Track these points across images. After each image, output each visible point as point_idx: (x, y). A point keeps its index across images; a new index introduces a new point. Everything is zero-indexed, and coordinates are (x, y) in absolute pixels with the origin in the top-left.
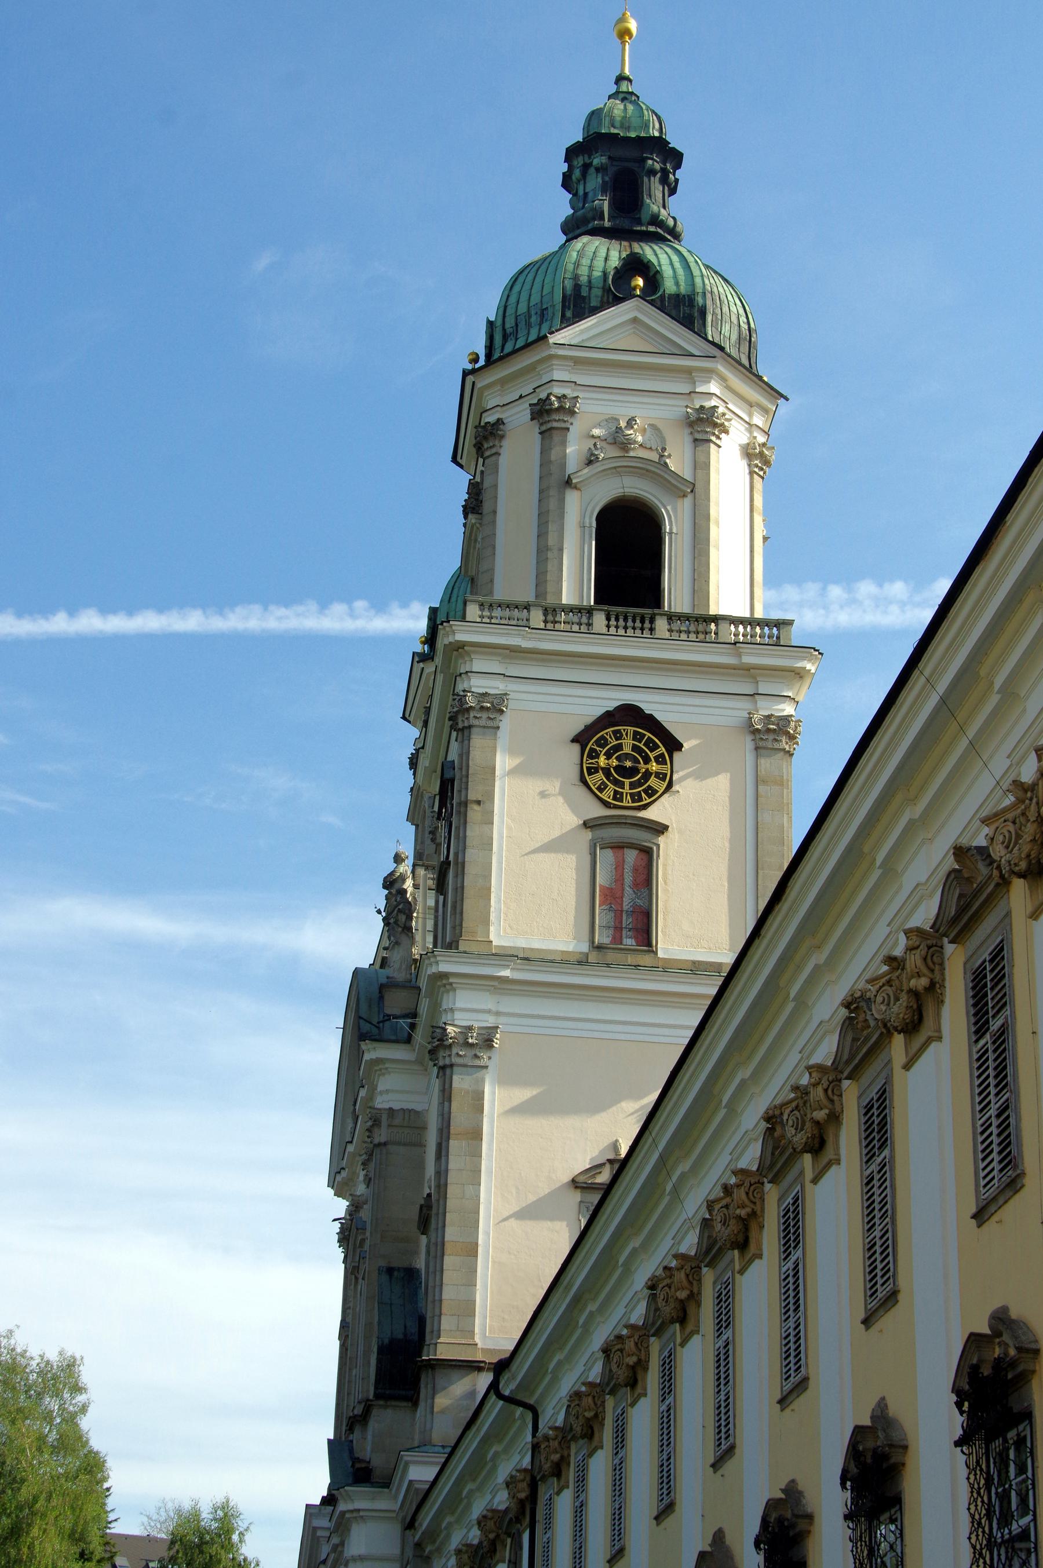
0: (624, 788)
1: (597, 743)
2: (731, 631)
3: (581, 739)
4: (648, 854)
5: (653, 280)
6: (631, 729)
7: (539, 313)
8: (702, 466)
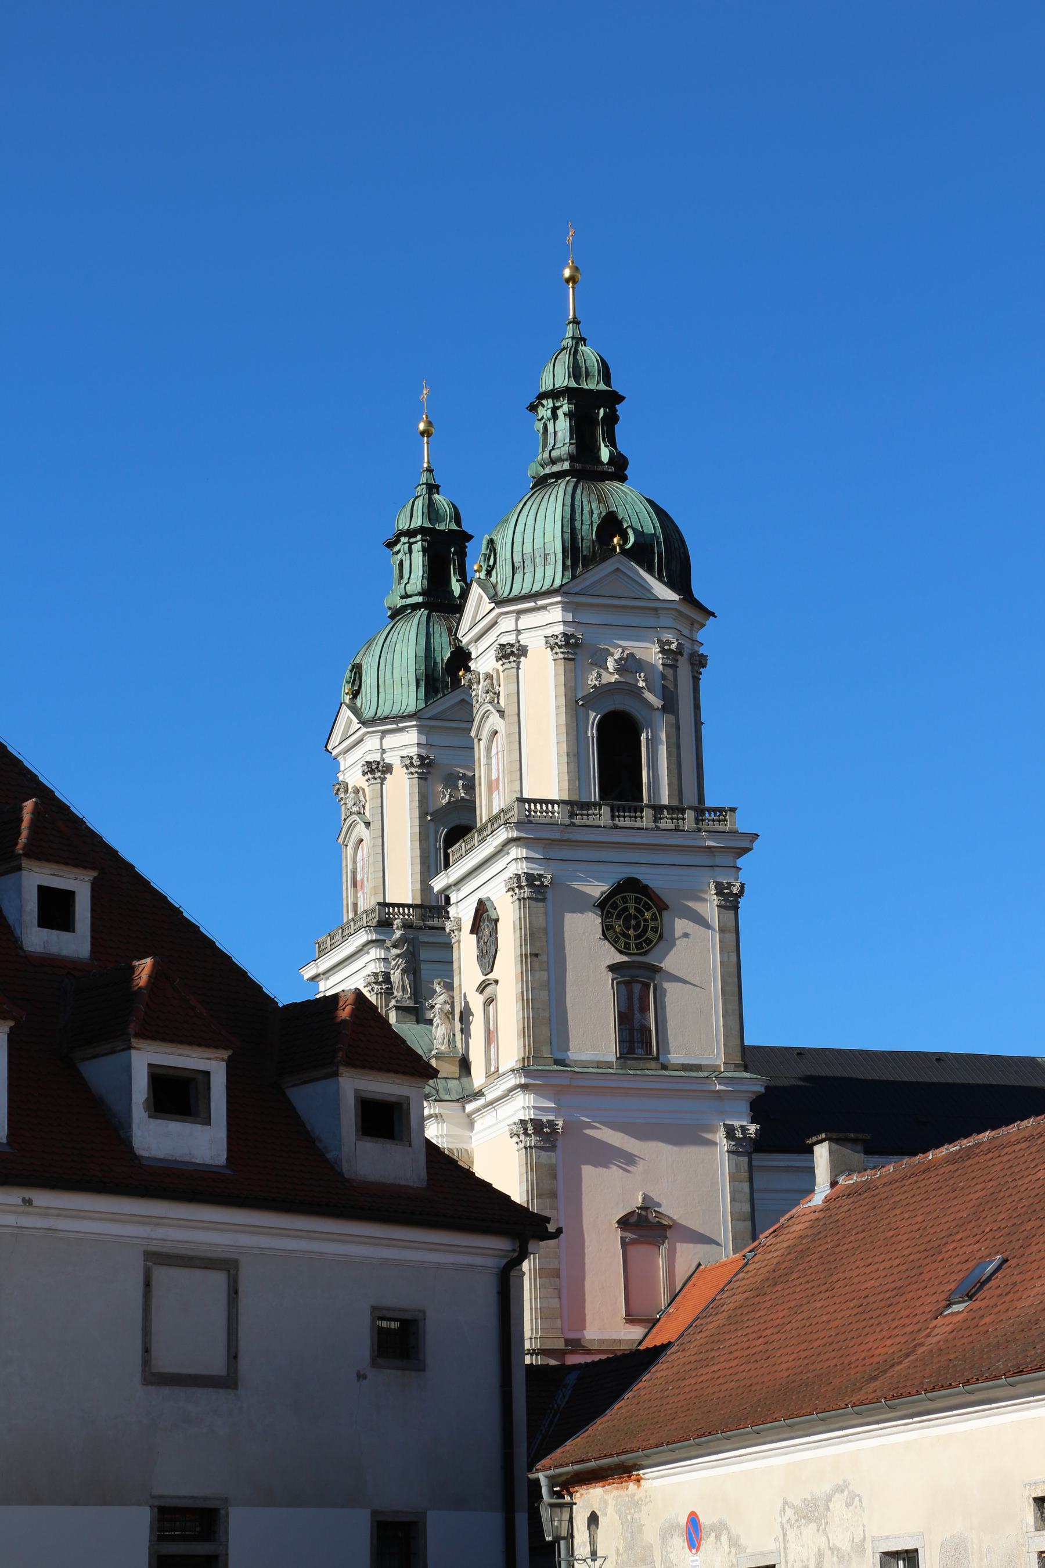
0: (630, 940)
7: (543, 556)
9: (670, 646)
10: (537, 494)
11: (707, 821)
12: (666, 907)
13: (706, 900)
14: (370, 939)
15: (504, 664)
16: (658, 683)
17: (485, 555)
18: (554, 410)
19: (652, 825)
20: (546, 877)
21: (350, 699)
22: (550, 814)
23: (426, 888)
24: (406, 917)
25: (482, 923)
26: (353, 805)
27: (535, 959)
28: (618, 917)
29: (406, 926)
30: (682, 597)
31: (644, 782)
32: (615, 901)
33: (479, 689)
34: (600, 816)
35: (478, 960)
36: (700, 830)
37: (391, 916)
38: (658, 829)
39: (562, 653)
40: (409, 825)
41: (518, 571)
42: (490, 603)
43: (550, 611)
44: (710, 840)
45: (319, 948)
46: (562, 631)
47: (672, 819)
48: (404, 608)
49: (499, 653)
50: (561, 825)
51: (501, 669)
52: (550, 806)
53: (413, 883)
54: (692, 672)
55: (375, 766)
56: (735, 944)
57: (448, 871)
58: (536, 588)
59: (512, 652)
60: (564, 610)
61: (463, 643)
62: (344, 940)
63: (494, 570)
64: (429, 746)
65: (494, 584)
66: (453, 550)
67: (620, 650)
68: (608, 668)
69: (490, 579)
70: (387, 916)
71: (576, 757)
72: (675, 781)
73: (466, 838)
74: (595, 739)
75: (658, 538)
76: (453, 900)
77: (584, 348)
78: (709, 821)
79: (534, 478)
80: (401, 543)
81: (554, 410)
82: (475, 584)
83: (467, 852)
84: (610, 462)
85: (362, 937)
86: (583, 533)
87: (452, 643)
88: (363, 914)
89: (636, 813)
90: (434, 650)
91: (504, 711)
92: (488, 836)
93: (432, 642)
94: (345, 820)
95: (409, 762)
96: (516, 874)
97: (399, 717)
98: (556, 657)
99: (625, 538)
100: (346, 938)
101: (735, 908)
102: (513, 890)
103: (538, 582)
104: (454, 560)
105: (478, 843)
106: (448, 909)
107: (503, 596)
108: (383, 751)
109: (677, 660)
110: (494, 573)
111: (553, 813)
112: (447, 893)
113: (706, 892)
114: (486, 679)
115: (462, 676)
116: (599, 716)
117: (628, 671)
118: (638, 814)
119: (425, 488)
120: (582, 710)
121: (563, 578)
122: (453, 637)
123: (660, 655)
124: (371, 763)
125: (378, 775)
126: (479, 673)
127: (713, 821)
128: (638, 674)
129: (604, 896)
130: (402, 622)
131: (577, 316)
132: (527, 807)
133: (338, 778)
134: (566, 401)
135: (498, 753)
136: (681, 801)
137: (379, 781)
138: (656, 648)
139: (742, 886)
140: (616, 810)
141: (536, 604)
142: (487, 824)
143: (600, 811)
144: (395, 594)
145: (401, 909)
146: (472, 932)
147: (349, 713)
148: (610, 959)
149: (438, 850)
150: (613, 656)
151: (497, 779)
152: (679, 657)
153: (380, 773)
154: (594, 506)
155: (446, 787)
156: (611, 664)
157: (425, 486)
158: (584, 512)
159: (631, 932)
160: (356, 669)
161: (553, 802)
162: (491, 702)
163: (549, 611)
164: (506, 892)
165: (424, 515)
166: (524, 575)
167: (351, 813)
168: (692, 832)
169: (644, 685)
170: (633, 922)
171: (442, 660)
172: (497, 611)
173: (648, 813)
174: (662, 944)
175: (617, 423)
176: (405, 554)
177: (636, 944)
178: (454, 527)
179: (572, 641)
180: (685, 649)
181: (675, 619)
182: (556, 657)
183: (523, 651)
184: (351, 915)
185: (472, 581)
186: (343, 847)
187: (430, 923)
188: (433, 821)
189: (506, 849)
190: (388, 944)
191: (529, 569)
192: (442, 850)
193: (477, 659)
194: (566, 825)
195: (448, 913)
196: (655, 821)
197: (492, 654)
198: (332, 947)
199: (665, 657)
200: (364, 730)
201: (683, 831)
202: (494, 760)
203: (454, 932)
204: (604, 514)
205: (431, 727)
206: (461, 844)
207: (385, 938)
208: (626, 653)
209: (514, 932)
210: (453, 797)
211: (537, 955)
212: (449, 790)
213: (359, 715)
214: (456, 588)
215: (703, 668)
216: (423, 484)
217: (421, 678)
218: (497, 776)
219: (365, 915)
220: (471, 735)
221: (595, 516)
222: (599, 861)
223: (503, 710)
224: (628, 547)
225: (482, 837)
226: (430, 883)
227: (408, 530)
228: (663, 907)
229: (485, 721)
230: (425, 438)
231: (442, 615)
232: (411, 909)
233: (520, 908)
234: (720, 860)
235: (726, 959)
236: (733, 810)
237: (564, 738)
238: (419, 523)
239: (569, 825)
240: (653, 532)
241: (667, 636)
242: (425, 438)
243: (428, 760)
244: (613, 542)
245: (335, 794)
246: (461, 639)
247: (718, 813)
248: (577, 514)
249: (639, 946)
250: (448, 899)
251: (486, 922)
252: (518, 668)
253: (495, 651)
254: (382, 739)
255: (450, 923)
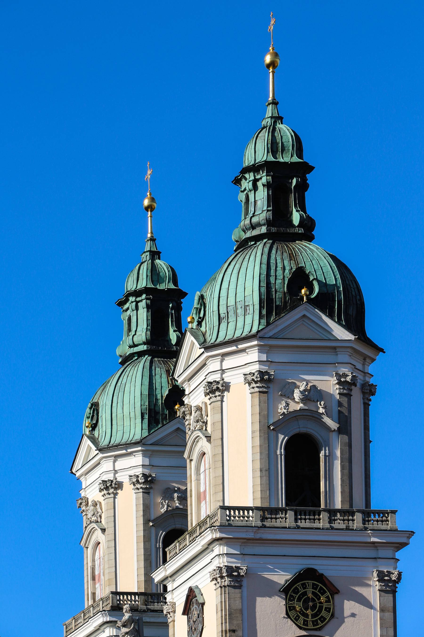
0: (308, 618)
1: (294, 591)
6: (310, 582)
7: (243, 307)
9: (345, 378)
10: (239, 255)
11: (372, 521)
12: (337, 592)
13: (369, 586)
14: (105, 621)
15: (211, 398)
16: (335, 409)
17: (197, 308)
18: (255, 182)
19: (327, 525)
20: (242, 569)
21: (89, 431)
22: (246, 518)
23: (148, 579)
24: (133, 603)
25: (191, 607)
26: (93, 516)
27: (233, 634)
28: (299, 600)
29: (133, 609)
30: (357, 337)
31: (321, 490)
32: (296, 587)
33: (191, 419)
34: (286, 519)
35: (188, 635)
36: (366, 529)
37: (122, 602)
38: (332, 528)
39: (258, 387)
40: (135, 530)
41: (223, 321)
42: (200, 348)
43: (249, 353)
44: (374, 537)
45: (66, 629)
46: (258, 369)
47: (344, 520)
48: (132, 355)
49: (207, 390)
50: (255, 527)
51: (208, 402)
52: (246, 512)
53: (138, 576)
54: (363, 399)
55: (110, 484)
56: (393, 621)
57: (166, 565)
58: (238, 334)
59: (218, 388)
60: (260, 351)
61: (179, 382)
62: (85, 621)
63: (204, 321)
64: (151, 466)
65: (203, 333)
66: (171, 305)
67: (305, 383)
68: (294, 399)
69: (201, 329)
70: (118, 602)
71: (268, 472)
72: (347, 489)
73: (179, 539)
74: (283, 457)
75: (338, 288)
76: (169, 589)
77: (281, 126)
78: (374, 521)
79: (237, 241)
80: (130, 302)
81: (255, 182)
82: (189, 333)
83: (181, 550)
84: (300, 225)
85: (99, 620)
86: (276, 287)
87: (170, 382)
88: (100, 601)
89: (314, 516)
90: (156, 389)
91: (211, 437)
92: (197, 537)
93: (154, 382)
94: (86, 527)
95: (135, 480)
96: (219, 567)
97: (128, 444)
98: (253, 390)
99: (311, 289)
100: (87, 620)
101: (394, 592)
102: (216, 580)
103: (239, 329)
104: (172, 314)
105: (189, 542)
106: (166, 596)
107: (210, 343)
108: (116, 472)
109: (351, 390)
110: (203, 324)
111: (248, 517)
112: (165, 583)
113: (370, 579)
114: (196, 411)
115: (178, 409)
116: (287, 438)
117: (311, 400)
118: (317, 517)
119: (149, 255)
120: (273, 434)
121: (259, 325)
122: (171, 378)
123: (338, 386)
124: (106, 481)
125: (111, 491)
126: (191, 406)
127: (377, 521)
128: (319, 403)
129: (288, 583)
130: (131, 367)
131: (275, 98)
132: (228, 513)
133: (81, 494)
134: (265, 174)
135: (205, 470)
136: (351, 505)
137: (112, 495)
138: (334, 380)
139: (400, 574)
140: (298, 514)
141: (237, 347)
142: (196, 527)
143: (285, 515)
144: (125, 344)
145: (129, 596)
146: (184, 613)
147: (89, 442)
148: (291, 633)
149: (157, 549)
150: (299, 388)
151: (205, 492)
152: (353, 387)
153: (113, 489)
154: (286, 263)
155: (164, 498)
156: (297, 395)
157: (148, 253)
158: (278, 269)
159: (309, 612)
160: (95, 407)
161: (248, 509)
162: (200, 430)
163: (248, 354)
164: (211, 581)
165: (148, 278)
166: (228, 324)
167: (91, 522)
168: (360, 530)
169: (324, 411)
170: (311, 604)
171: (162, 396)
172: (206, 355)
173: (324, 516)
174: (334, 621)
175: (306, 190)
176: (133, 311)
177: (312, 621)
178: (172, 286)
179: (266, 377)
180: (359, 381)
181: (350, 356)
182: (253, 390)
183: (226, 387)
184: (91, 602)
185: (186, 331)
186: (85, 549)
187: (151, 607)
188: (154, 526)
189: (211, 547)
190: (119, 624)
191: (232, 319)
192: (161, 549)
193: (190, 395)
194: (258, 527)
195: (165, 598)
196: (330, 522)
197: (201, 390)
198: (76, 628)
199: (341, 387)
200: (101, 455)
201: (352, 530)
202: (202, 476)
203: (170, 614)
204: (294, 270)
205: (153, 451)
206: (176, 543)
207: (117, 620)
208: (309, 386)
209: (217, 613)
210: (170, 507)
211: (234, 631)
212: (167, 501)
213: (97, 443)
214: (173, 337)
215: (372, 395)
216: (147, 252)
217: (145, 412)
218: (204, 489)
219: (101, 602)
220: (185, 457)
221: (287, 271)
222: (285, 556)
223: (210, 436)
224: (313, 296)
225: (192, 538)
226: (151, 575)
227: (135, 291)
228: (335, 591)
229: (196, 445)
230: (149, 212)
231: (162, 360)
232: (137, 596)
233: (221, 594)
234: (382, 553)
235: (385, 633)
236: (394, 512)
237: (258, 456)
238: (144, 285)
239: (261, 527)
240: (335, 283)
241: (343, 370)
242: (149, 212)
243: (150, 478)
244: (301, 292)
245: (78, 508)
246: (177, 379)
247: (381, 515)
248: (272, 271)
249: (315, 623)
250: (165, 587)
251: (195, 606)
252: (222, 401)
253: (204, 387)
254: (114, 462)
255: (167, 606)
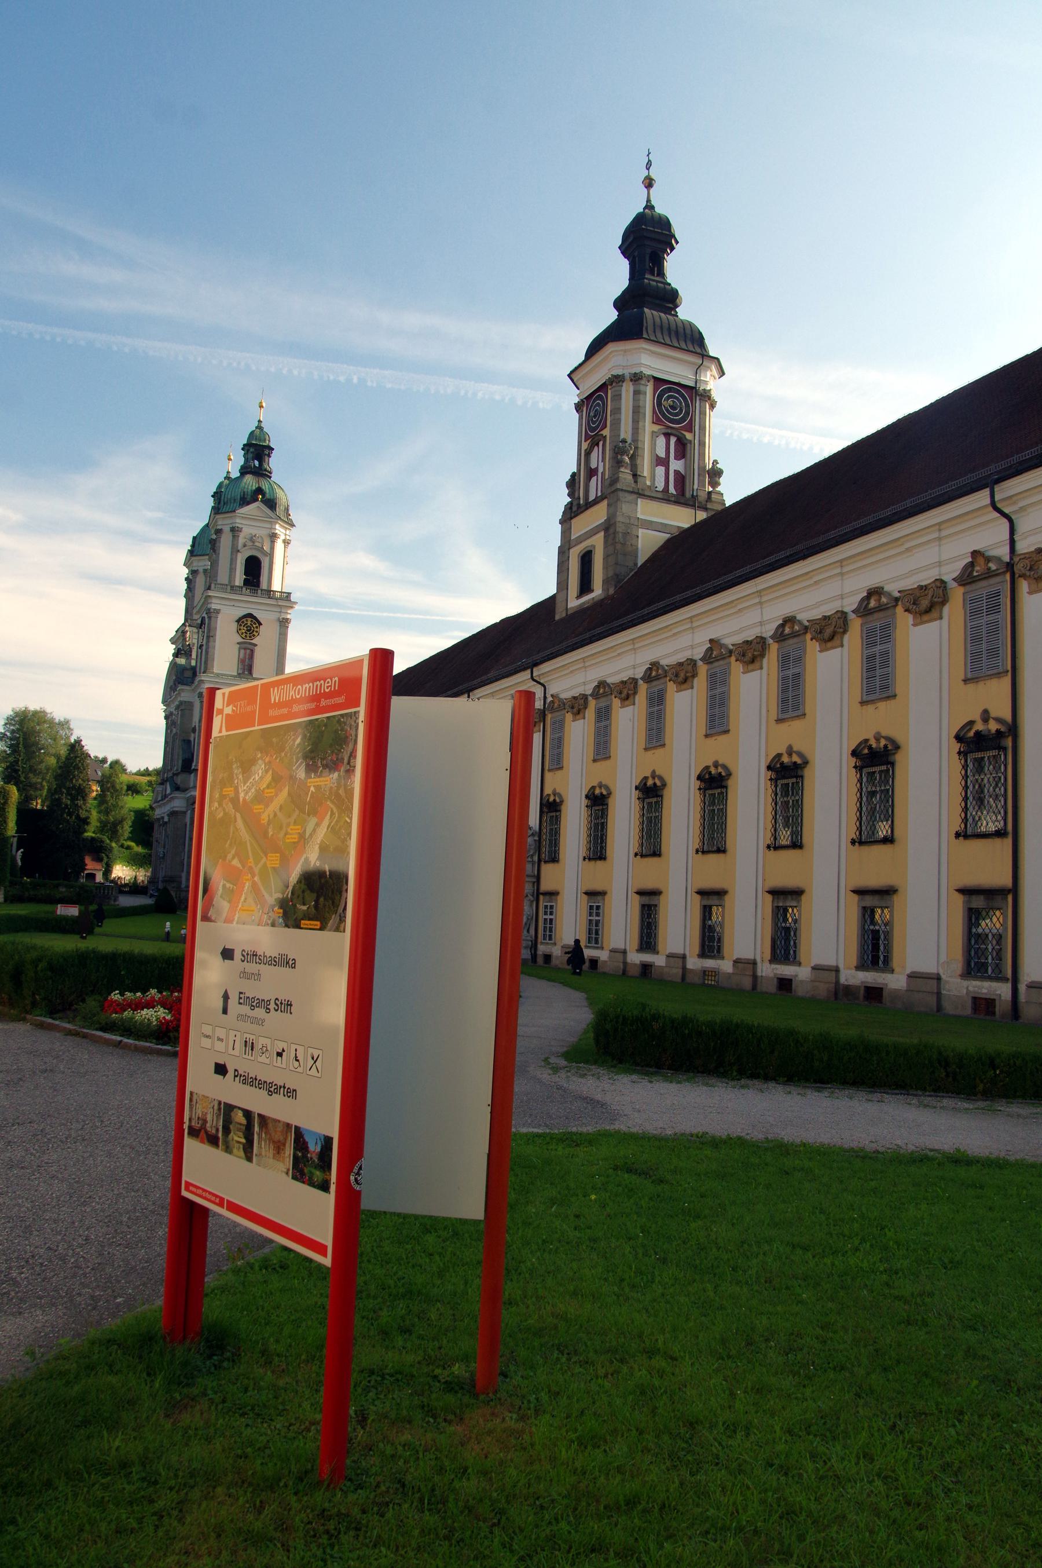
2: (278, 595)
3: (238, 621)
4: (252, 651)
5: (264, 494)
8: (272, 548)
